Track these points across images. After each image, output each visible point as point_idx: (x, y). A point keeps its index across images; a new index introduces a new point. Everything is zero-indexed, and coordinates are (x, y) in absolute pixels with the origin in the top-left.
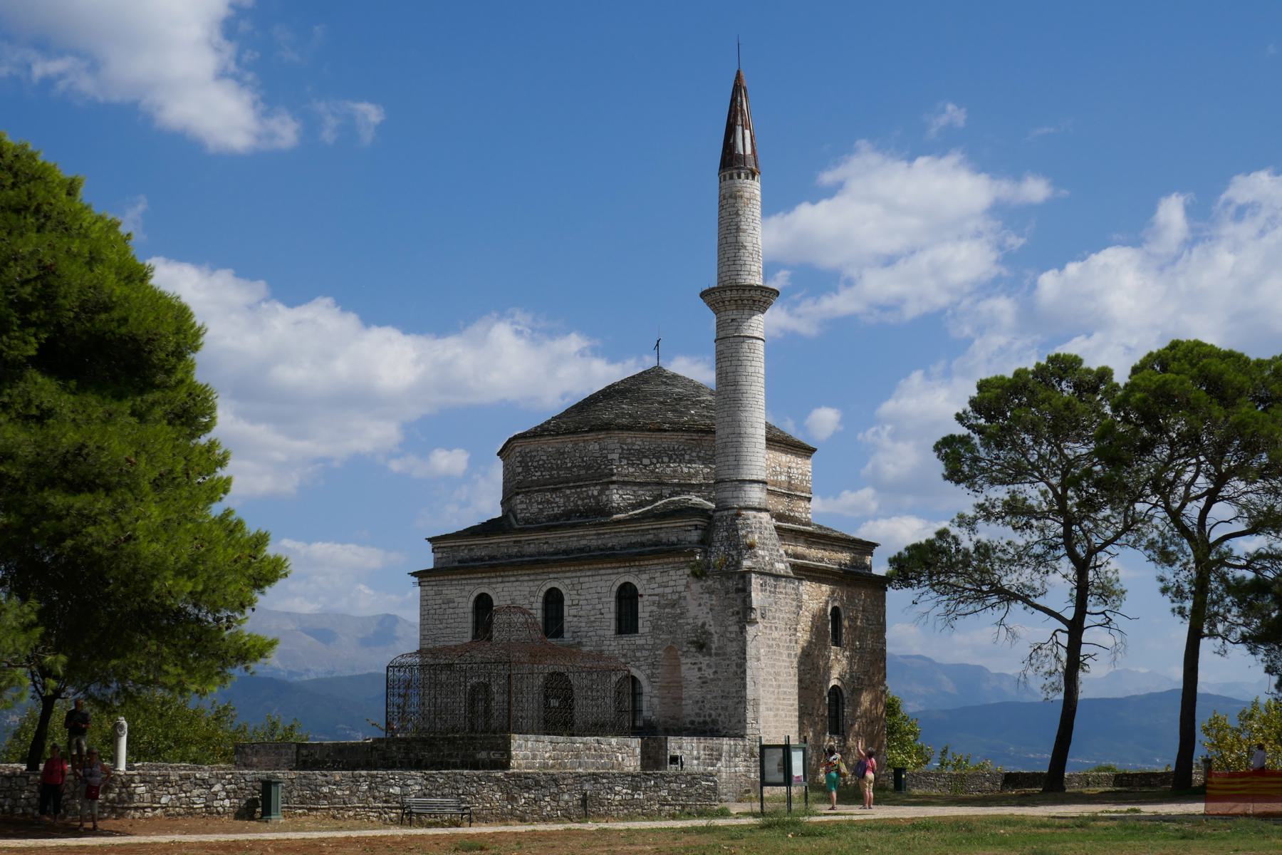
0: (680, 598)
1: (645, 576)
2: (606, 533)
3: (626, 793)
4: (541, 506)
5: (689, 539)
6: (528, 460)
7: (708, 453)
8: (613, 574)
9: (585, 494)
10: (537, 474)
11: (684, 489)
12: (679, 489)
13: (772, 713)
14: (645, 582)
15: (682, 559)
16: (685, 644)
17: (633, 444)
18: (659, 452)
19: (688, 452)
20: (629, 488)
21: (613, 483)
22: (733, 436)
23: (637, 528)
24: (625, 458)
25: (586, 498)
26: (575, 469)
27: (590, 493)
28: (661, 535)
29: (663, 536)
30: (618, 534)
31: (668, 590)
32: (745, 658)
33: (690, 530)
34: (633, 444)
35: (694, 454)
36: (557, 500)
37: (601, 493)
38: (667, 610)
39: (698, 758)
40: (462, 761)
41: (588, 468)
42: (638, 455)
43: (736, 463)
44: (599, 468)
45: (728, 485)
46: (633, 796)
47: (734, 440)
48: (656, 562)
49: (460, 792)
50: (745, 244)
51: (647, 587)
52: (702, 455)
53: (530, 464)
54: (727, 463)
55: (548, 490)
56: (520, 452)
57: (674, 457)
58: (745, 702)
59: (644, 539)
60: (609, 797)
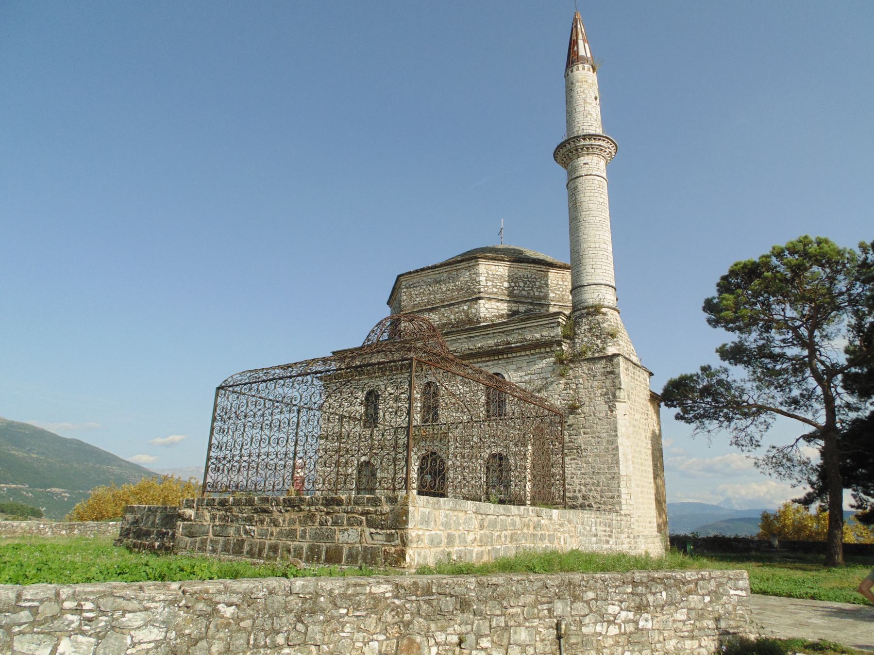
2: (475, 336)
3: (627, 621)
7: (553, 282)
10: (417, 299)
11: (536, 307)
12: (532, 307)
13: (639, 489)
17: (496, 271)
18: (517, 278)
19: (539, 280)
20: (493, 303)
21: (480, 298)
23: (503, 330)
25: (457, 313)
30: (486, 336)
32: (616, 435)
35: (543, 282)
37: (470, 307)
39: (596, 536)
40: (311, 549)
42: (501, 279)
43: (593, 270)
46: (636, 623)
47: (591, 252)
48: (523, 353)
49: (280, 639)
50: (591, 112)
55: (426, 310)
57: (528, 283)
58: (619, 478)
60: (599, 629)
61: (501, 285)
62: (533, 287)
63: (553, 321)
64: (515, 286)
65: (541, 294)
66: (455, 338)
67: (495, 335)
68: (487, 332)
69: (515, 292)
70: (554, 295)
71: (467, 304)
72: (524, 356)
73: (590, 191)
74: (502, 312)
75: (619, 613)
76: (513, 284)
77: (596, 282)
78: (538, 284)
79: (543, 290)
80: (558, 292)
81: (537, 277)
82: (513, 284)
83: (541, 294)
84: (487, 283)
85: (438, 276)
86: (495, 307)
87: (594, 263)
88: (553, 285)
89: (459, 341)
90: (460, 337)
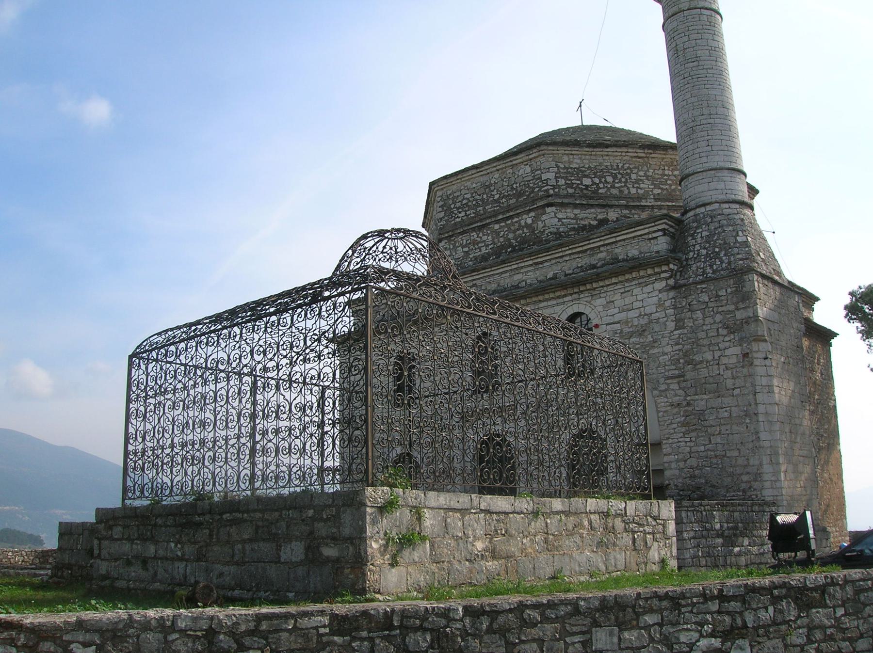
0: (650, 322)
1: (600, 302)
2: (546, 261)
4: (466, 249)
5: (656, 248)
6: (451, 202)
7: (657, 172)
8: (557, 304)
9: (517, 224)
10: (460, 215)
11: (633, 211)
12: (628, 212)
14: (600, 309)
15: (650, 271)
16: (662, 380)
17: (570, 162)
18: (602, 170)
20: (568, 210)
22: (701, 117)
23: (584, 248)
24: (562, 178)
25: (518, 230)
26: (504, 200)
27: (523, 223)
28: (617, 251)
29: (620, 252)
31: (632, 314)
33: (656, 238)
34: (570, 162)
36: (485, 238)
37: (536, 219)
38: (633, 340)
41: (520, 194)
44: (533, 192)
45: (701, 175)
48: (614, 280)
51: (603, 314)
52: (650, 174)
53: (452, 206)
54: (698, 150)
56: (441, 196)
57: (619, 176)
59: (593, 260)
61: (579, 182)
62: (626, 182)
63: (655, 228)
64: (601, 182)
65: (640, 191)
66: (516, 266)
67: (573, 256)
68: (561, 254)
69: (600, 191)
70: (660, 191)
71: (530, 215)
72: (616, 283)
73: (696, 32)
74: (583, 223)
75: (698, 641)
76: (597, 180)
77: (714, 165)
78: (634, 176)
79: (642, 186)
80: (664, 187)
81: (631, 166)
82: (597, 180)
83: (640, 191)
84: (557, 181)
85: (485, 178)
86: (572, 216)
87: (709, 137)
88: (657, 176)
89: (522, 271)
90: (523, 264)
